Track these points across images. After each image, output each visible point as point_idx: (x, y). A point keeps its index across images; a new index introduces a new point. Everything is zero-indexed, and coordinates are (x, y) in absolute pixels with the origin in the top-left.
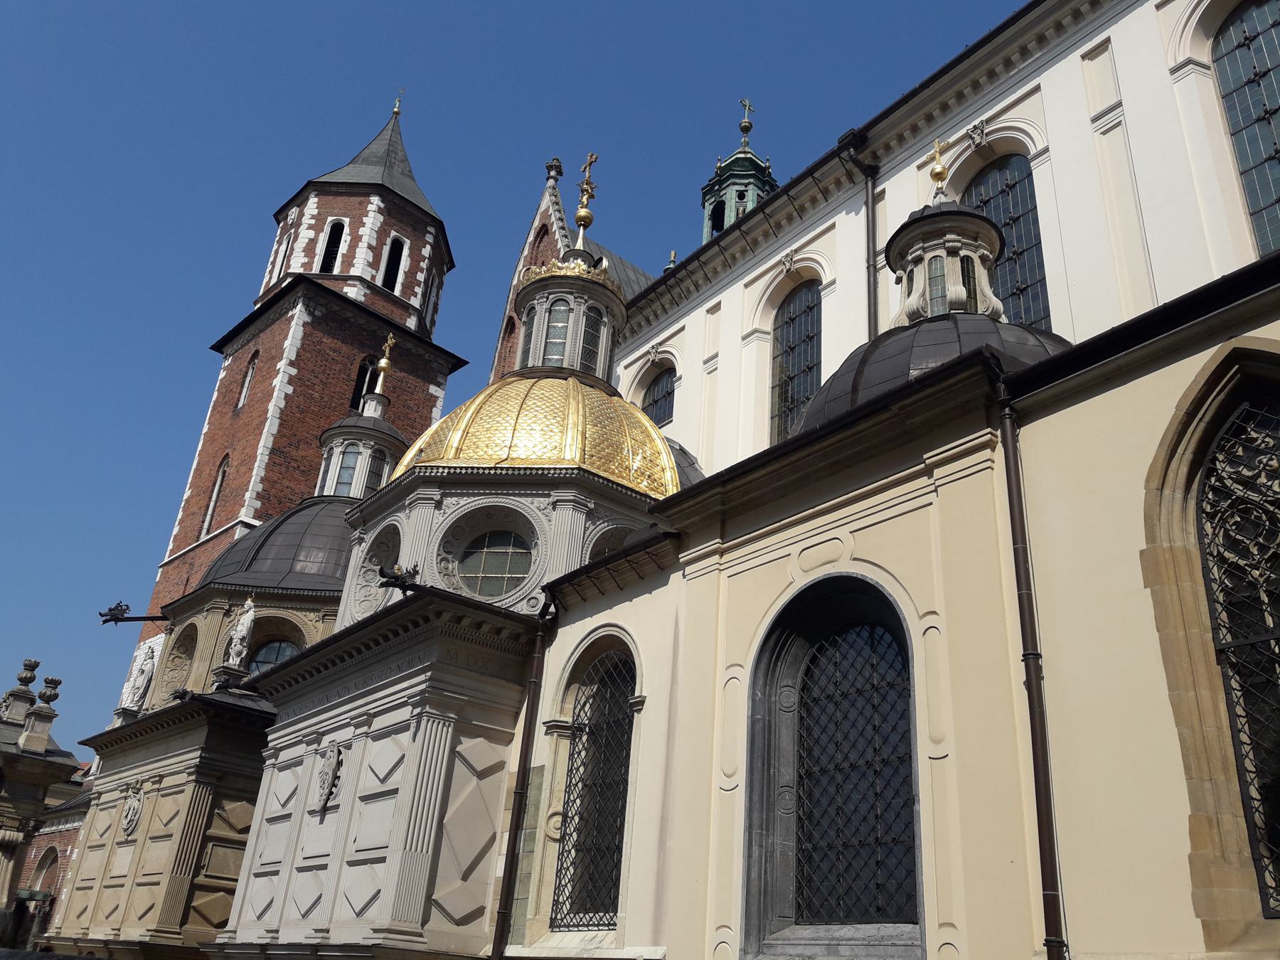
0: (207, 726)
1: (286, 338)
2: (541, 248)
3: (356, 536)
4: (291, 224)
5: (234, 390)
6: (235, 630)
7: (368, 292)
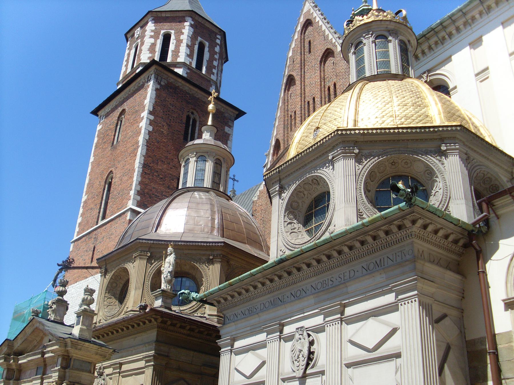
0: (156, 329)
1: (145, 98)
2: (306, 33)
3: (277, 189)
5: (110, 134)
6: (164, 267)
7: (189, 71)
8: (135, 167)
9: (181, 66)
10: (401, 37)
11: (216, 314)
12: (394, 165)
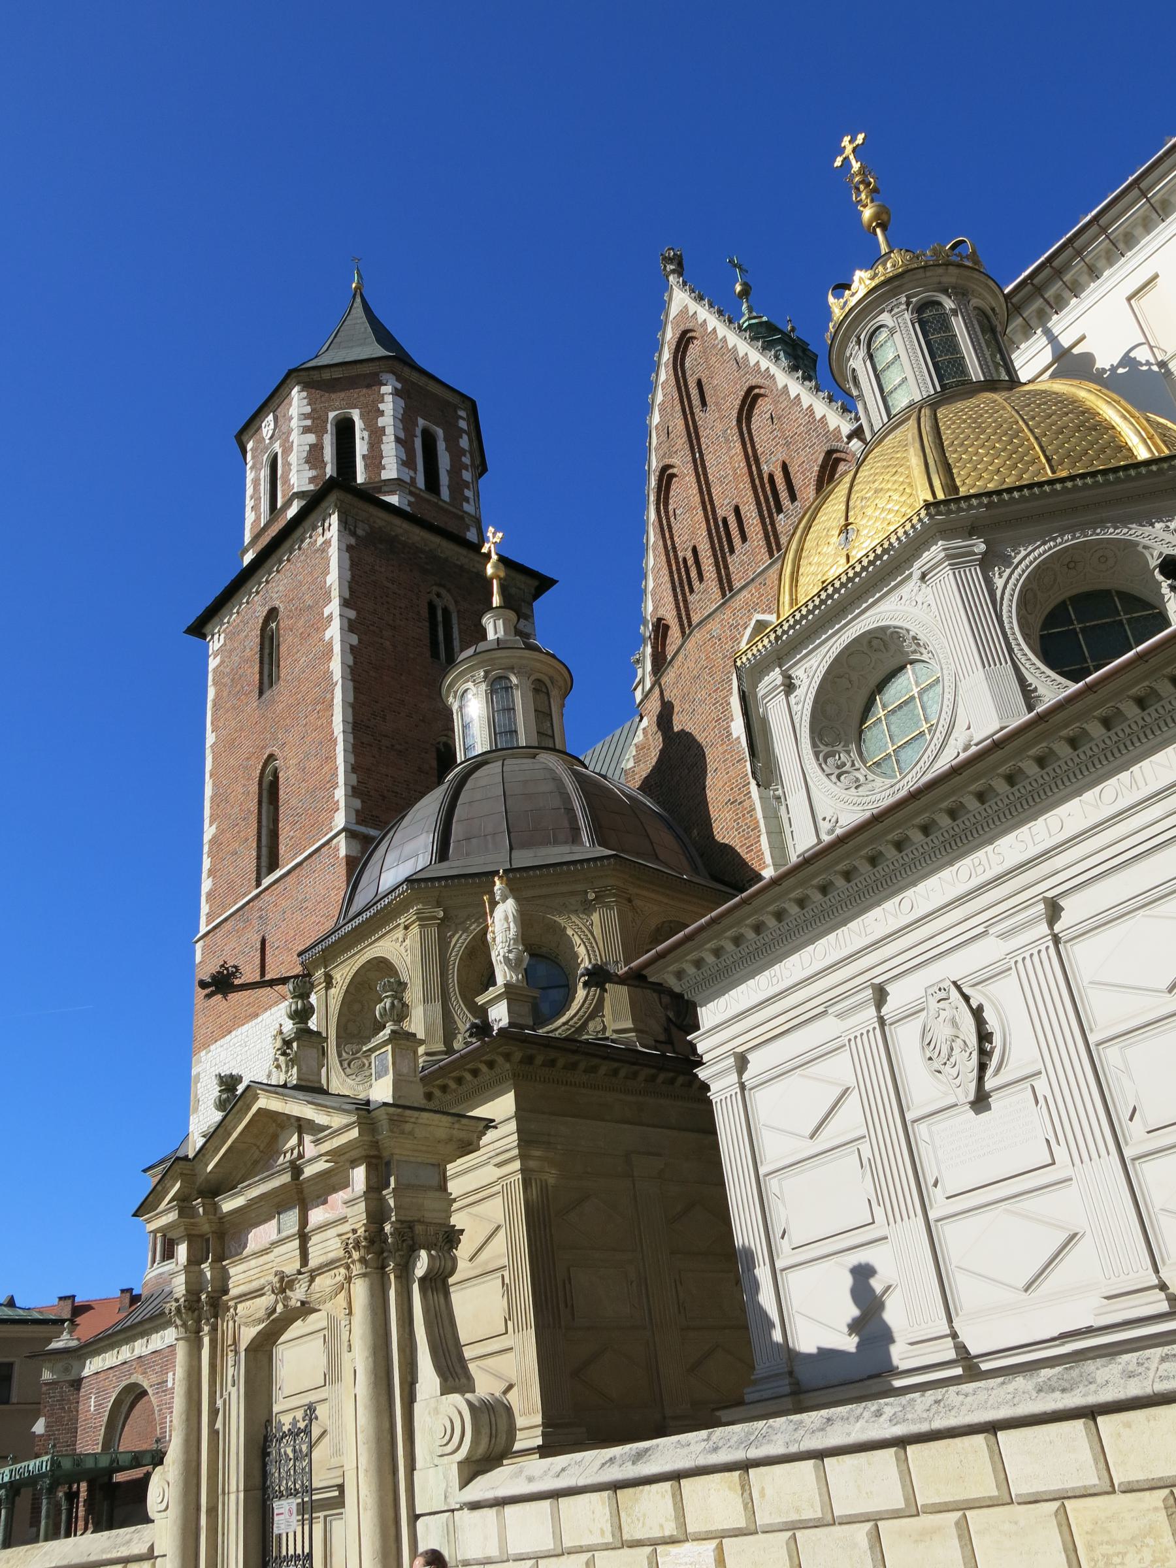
1: (326, 572)
4: (271, 438)
7: (412, 499)
8: (335, 734)
9: (392, 488)
10: (974, 302)
11: (632, 1026)
12: (1074, 568)
